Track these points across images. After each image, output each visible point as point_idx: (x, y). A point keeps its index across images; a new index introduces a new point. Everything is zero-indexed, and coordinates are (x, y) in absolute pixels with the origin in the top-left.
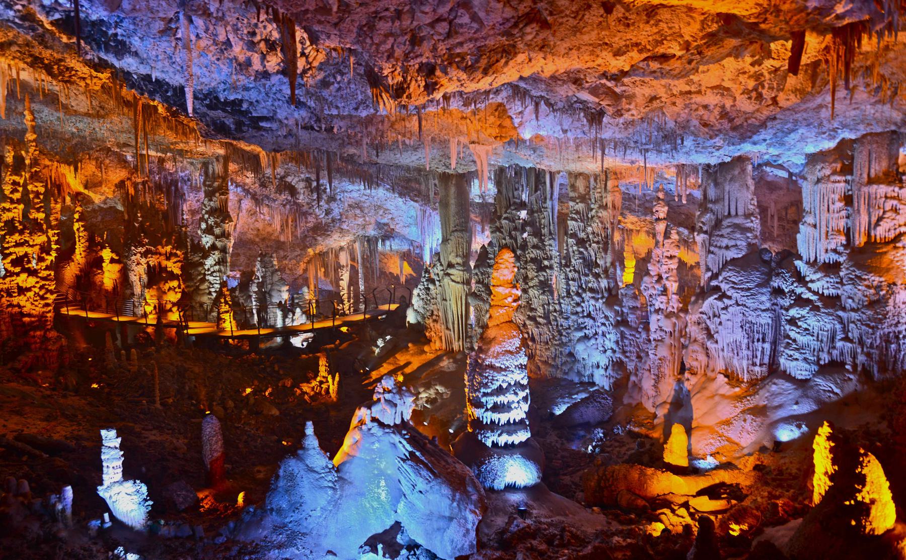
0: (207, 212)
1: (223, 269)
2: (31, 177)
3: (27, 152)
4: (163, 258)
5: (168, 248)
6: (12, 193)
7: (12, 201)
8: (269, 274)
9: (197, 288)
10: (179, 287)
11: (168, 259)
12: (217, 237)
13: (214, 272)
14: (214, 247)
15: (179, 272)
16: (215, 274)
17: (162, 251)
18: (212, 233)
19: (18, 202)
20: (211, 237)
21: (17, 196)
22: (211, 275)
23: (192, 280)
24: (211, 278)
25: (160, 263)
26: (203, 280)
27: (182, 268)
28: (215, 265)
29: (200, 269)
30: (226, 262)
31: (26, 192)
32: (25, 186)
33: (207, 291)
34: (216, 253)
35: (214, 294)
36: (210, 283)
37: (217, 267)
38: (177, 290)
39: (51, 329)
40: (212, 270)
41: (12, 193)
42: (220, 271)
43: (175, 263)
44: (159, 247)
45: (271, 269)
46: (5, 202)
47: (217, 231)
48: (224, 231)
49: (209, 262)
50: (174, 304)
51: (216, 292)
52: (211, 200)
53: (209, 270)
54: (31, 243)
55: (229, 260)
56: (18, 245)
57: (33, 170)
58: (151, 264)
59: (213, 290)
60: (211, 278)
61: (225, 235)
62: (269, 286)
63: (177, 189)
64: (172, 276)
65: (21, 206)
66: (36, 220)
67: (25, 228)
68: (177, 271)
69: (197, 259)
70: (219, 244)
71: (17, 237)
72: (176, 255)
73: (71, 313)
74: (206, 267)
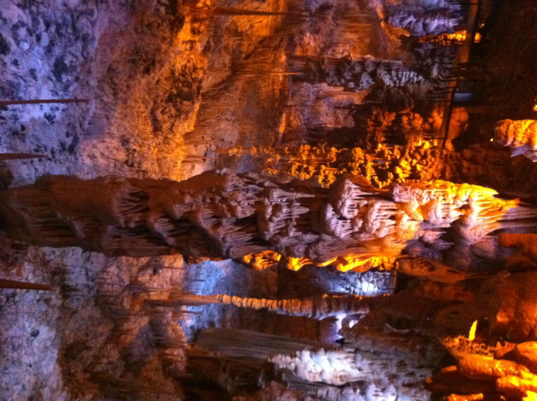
0: (339, 80)
1: (396, 67)
2: (294, 155)
3: (268, 156)
4: (378, 128)
5: (370, 123)
6: (308, 173)
7: (318, 173)
8: (407, 9)
9: (413, 96)
10: (408, 115)
11: (379, 124)
12: (364, 70)
13: (397, 76)
14: (373, 75)
15: (394, 114)
16: (400, 76)
17: (371, 129)
18: (360, 75)
20: (363, 76)
22: (400, 80)
23: (403, 100)
24: (404, 80)
25: (384, 132)
26: (405, 89)
27: (391, 111)
28: (391, 74)
29: (393, 92)
30: (389, 63)
33: (416, 86)
34: (379, 71)
35: (421, 78)
36: (408, 82)
37: (393, 73)
38: (411, 118)
40: (395, 79)
41: (308, 173)
42: (397, 70)
43: (384, 118)
44: (368, 130)
45: (402, 6)
46: (317, 179)
47: (358, 69)
48: (359, 62)
49: (387, 81)
50: (425, 121)
51: (417, 76)
52: (328, 75)
53: (395, 83)
54: (363, 162)
55: (387, 61)
56: (364, 172)
57: (287, 152)
58: (383, 139)
59: (415, 79)
60: (404, 80)
61: (362, 63)
62: (420, 8)
63: (315, 130)
64: (398, 121)
66: (338, 155)
68: (393, 117)
69: (383, 95)
70: (370, 69)
72: (377, 116)
74: (392, 85)
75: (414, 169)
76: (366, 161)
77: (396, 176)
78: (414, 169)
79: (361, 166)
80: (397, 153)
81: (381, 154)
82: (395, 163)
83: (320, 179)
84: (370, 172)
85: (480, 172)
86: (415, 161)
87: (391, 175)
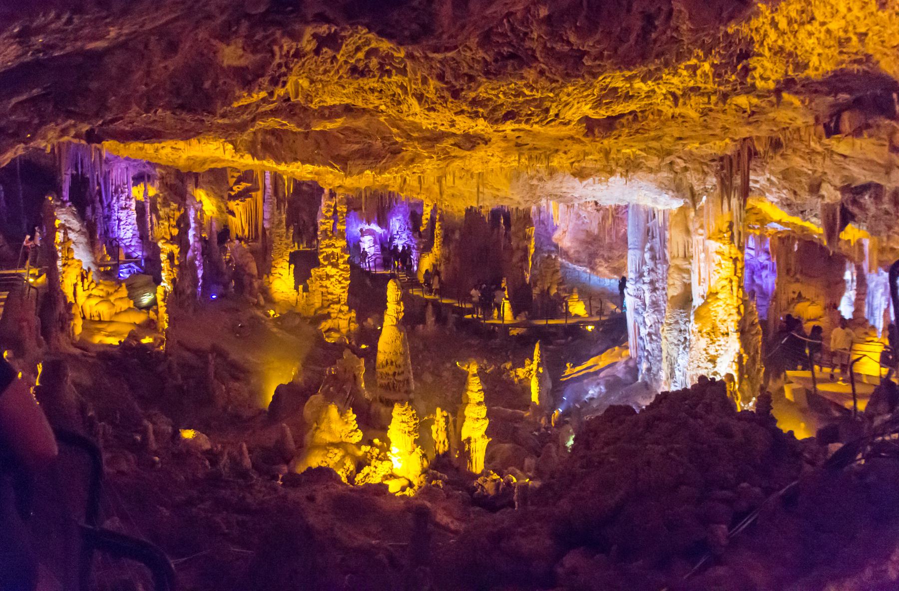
7: (327, 218)
19: (330, 218)
21: (330, 214)
31: (335, 212)
32: (335, 206)
37: (520, 264)
39: (345, 304)
56: (328, 246)
65: (332, 221)
67: (333, 235)
71: (327, 241)
73: (415, 293)
75: (332, 276)
76: (335, 247)
77: (326, 266)
78: (332, 276)
79: (333, 244)
80: (342, 267)
81: (342, 257)
82: (335, 266)
83: (323, 221)
84: (329, 250)
85: (332, 315)
86: (337, 277)
87: (326, 263)
